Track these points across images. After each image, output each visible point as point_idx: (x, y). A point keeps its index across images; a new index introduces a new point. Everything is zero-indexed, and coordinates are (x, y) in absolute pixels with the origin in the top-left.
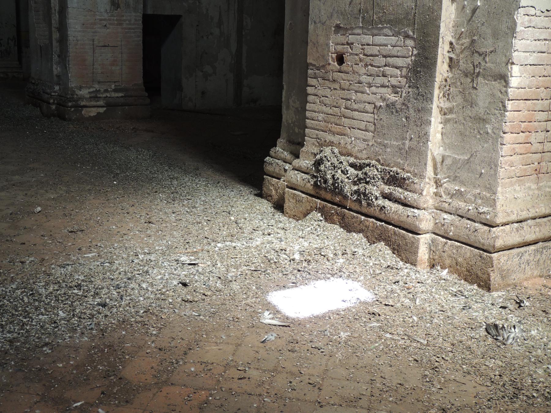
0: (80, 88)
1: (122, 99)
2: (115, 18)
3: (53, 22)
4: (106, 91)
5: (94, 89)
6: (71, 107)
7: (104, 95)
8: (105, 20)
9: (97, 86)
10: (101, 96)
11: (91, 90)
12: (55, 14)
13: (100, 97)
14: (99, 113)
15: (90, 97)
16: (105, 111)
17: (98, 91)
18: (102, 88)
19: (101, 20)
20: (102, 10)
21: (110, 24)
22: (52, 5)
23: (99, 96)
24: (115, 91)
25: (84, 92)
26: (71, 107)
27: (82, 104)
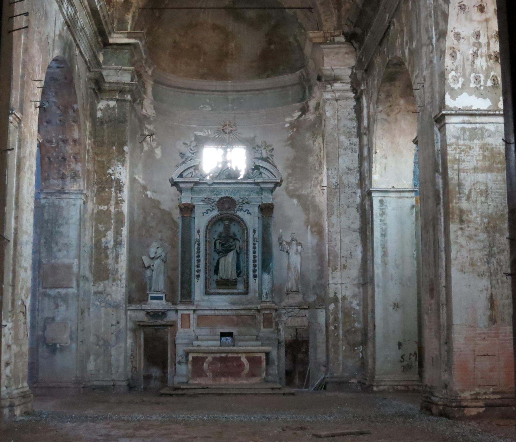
0: (463, 391)
1: (499, 400)
2: (493, 332)
3: (442, 337)
4: (485, 393)
5: (475, 392)
6: (455, 407)
7: (484, 397)
8: (484, 333)
9: (477, 390)
10: (481, 397)
11: (472, 393)
12: (444, 330)
13: (479, 399)
14: (479, 413)
15: (472, 399)
16: (484, 411)
17: (478, 394)
18: (482, 391)
19: (481, 334)
20: (482, 325)
21: (489, 337)
22: (441, 323)
23: (478, 397)
24: (494, 393)
25: (467, 395)
26: (455, 407)
27: (464, 404)
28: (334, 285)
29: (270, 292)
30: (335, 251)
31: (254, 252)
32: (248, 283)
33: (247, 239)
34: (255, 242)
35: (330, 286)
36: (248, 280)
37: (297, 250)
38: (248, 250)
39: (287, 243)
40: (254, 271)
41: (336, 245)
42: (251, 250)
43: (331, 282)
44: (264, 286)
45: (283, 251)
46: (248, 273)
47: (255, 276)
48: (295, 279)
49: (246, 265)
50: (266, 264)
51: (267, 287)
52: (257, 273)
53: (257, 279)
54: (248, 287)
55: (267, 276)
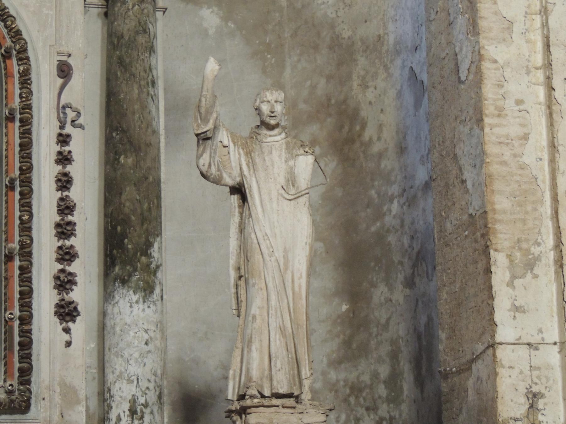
28: (523, 351)
29: (152, 397)
30: (523, 167)
31: (64, 182)
32: (26, 345)
33: (27, 107)
34: (69, 129)
35: (504, 354)
36: (26, 334)
37: (291, 179)
38: (26, 171)
39: (234, 137)
40: (64, 282)
41: (526, 137)
42: (45, 172)
43: (505, 332)
44: (116, 365)
45: (217, 181)
46: (26, 296)
47: (66, 312)
48: (282, 330)
49: (15, 245)
50: (128, 250)
51: (133, 369)
52: (76, 295)
53: (78, 327)
54: (26, 373)
55: (138, 309)
